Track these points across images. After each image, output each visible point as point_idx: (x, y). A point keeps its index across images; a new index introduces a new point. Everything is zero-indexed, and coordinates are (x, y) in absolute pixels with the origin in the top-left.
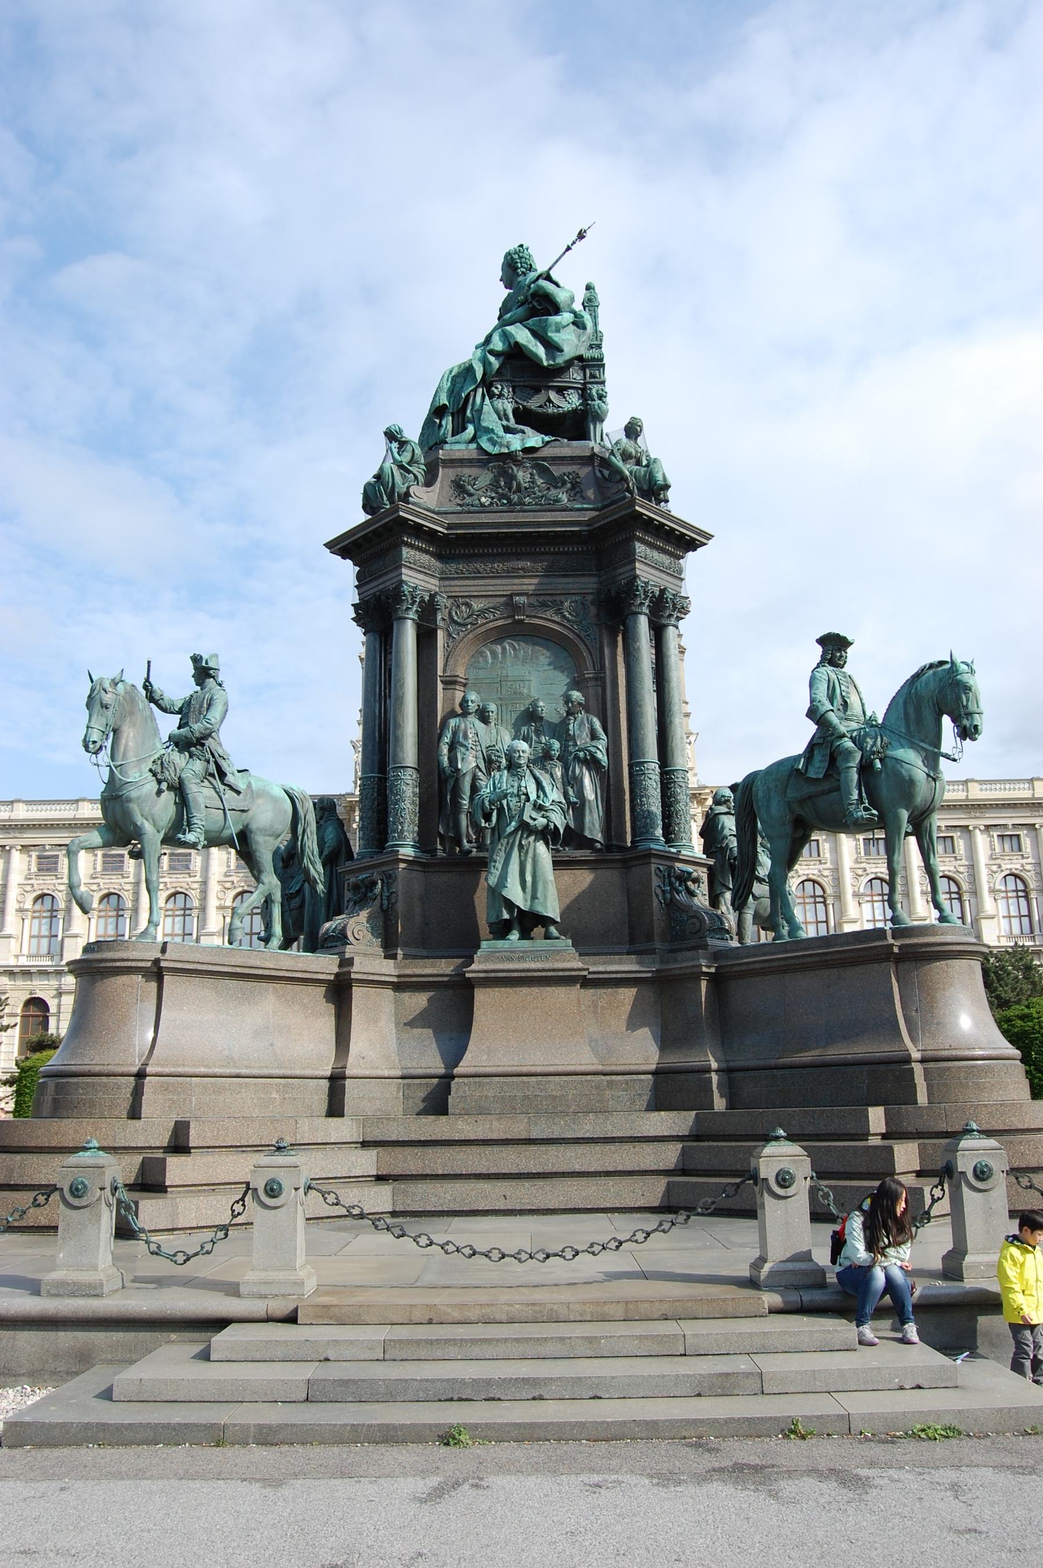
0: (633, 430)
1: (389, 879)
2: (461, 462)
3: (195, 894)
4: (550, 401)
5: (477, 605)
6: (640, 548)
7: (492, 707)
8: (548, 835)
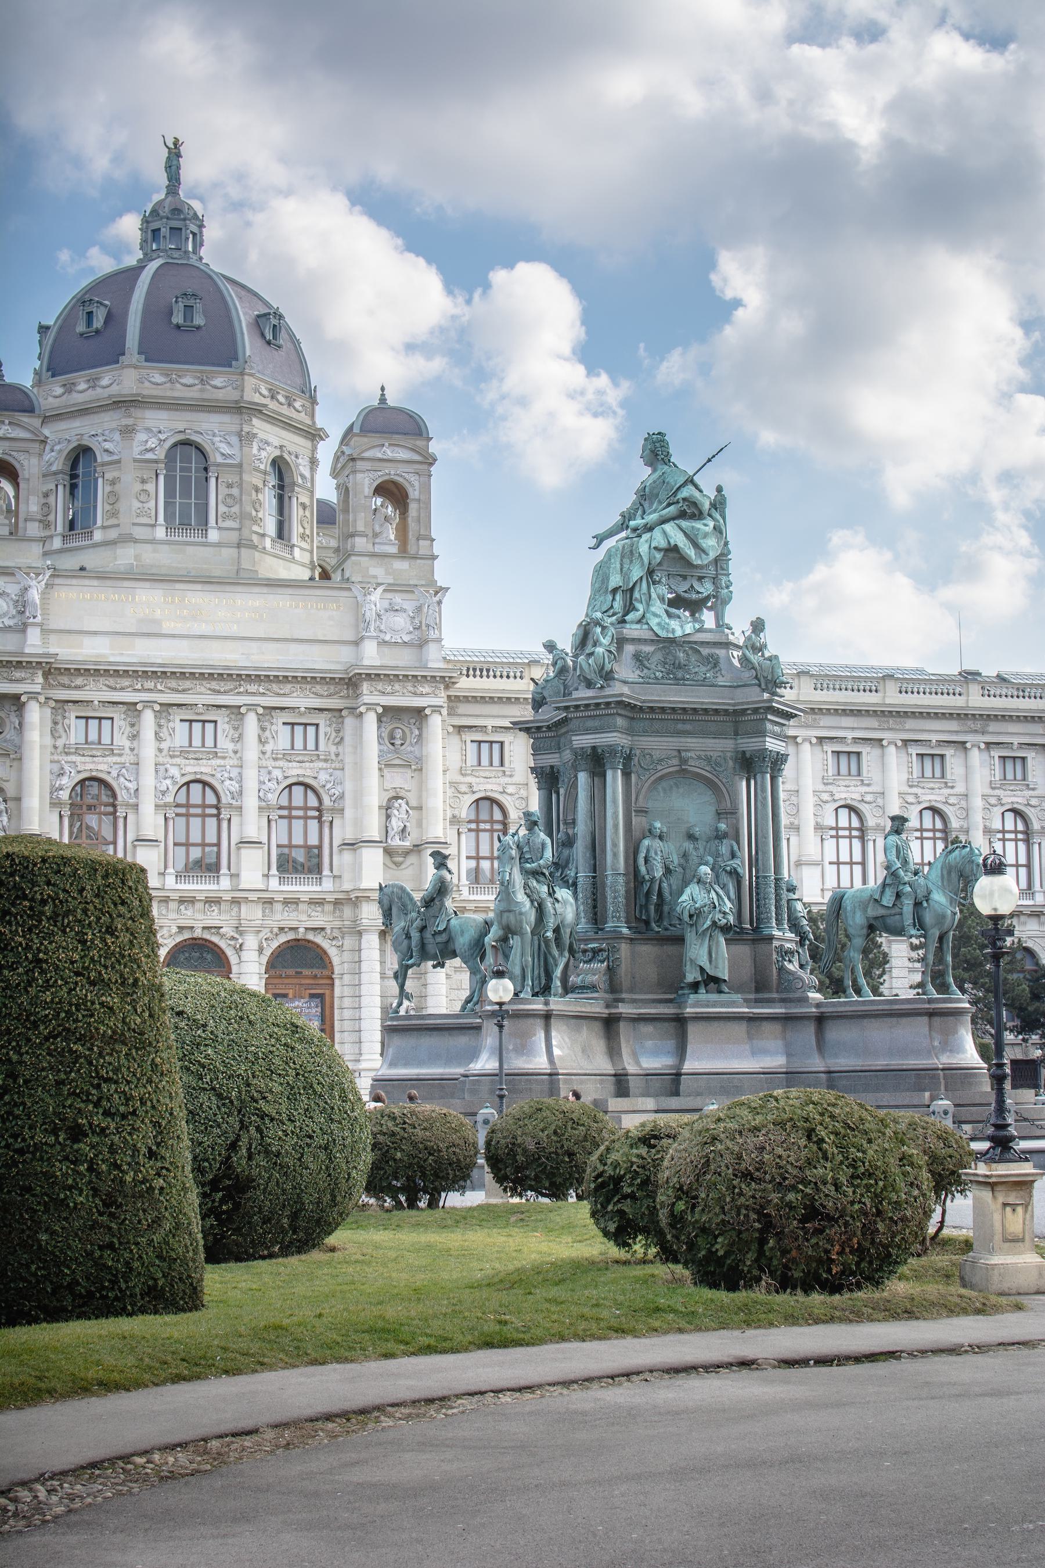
1: (614, 950)
4: (692, 586)
6: (769, 726)
8: (726, 929)
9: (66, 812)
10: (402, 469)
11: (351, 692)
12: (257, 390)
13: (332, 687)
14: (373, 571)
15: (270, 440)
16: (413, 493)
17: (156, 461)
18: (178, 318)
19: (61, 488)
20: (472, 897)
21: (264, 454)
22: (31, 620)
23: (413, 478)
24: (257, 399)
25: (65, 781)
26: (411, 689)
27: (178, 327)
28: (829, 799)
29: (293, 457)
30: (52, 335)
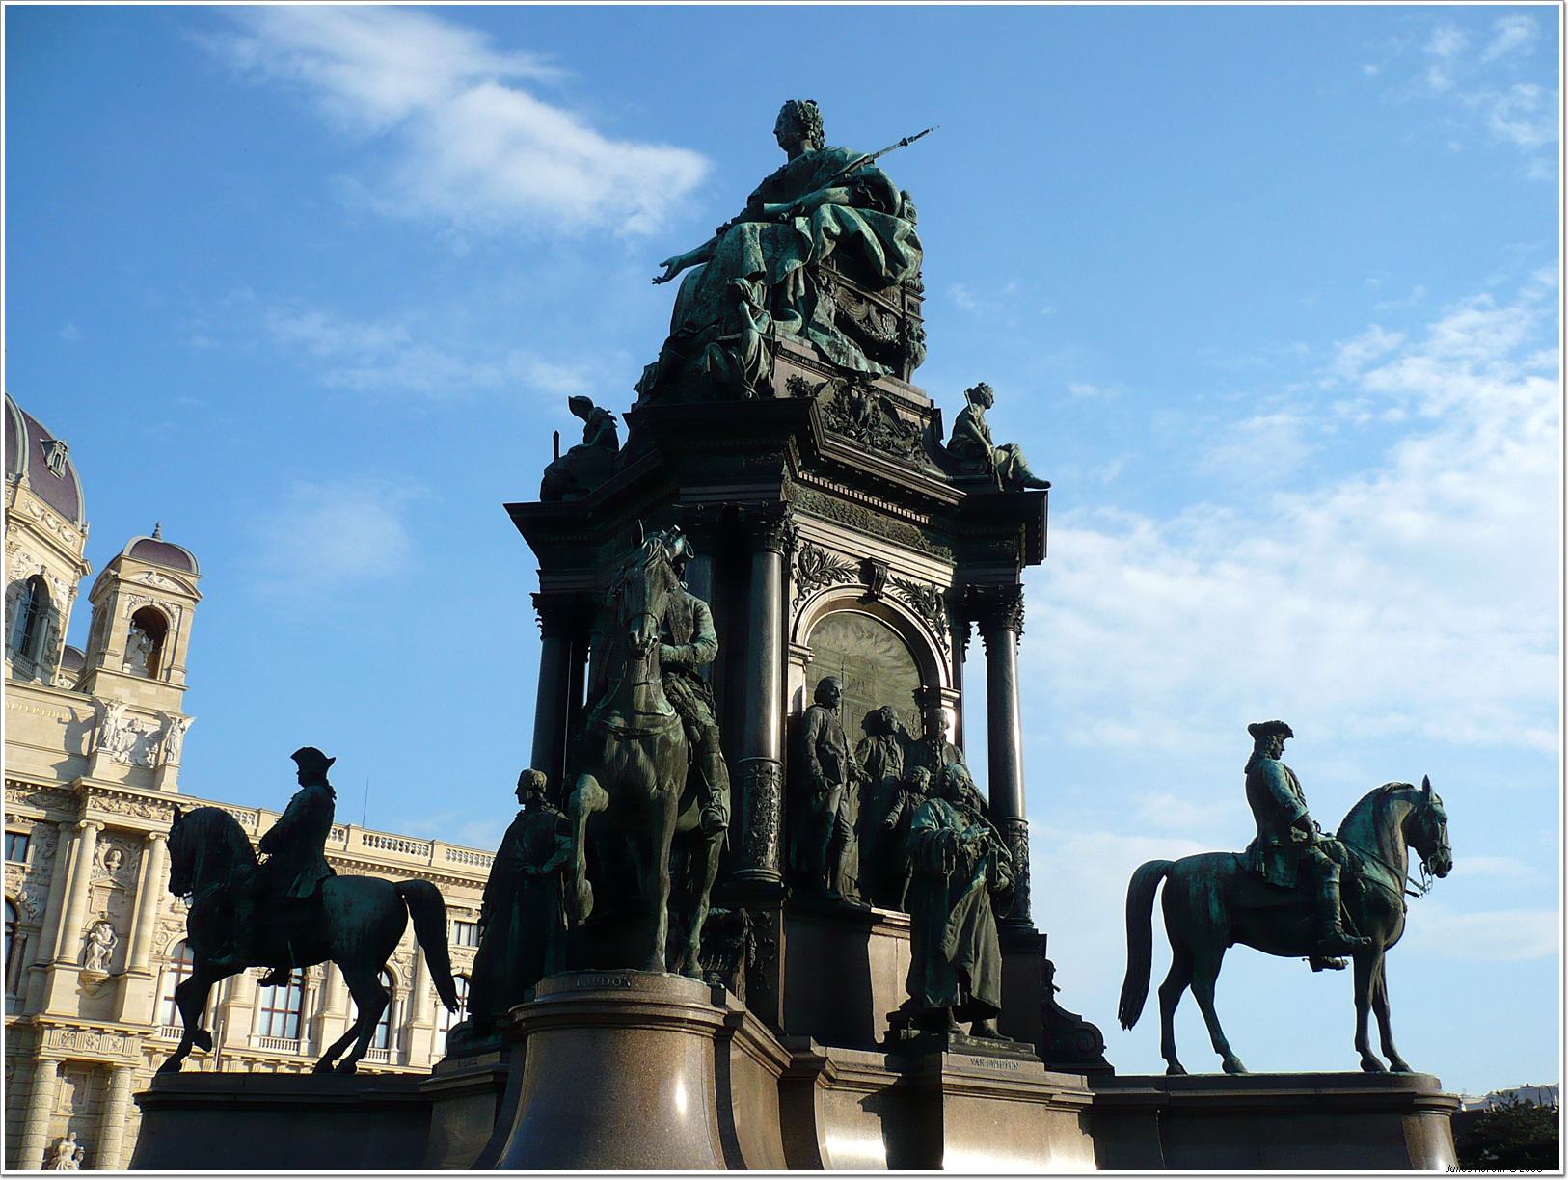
10: (166, 598)
11: (73, 806)
12: (28, 506)
13: (53, 798)
15: (32, 557)
21: (23, 567)
23: (174, 609)
29: (53, 580)
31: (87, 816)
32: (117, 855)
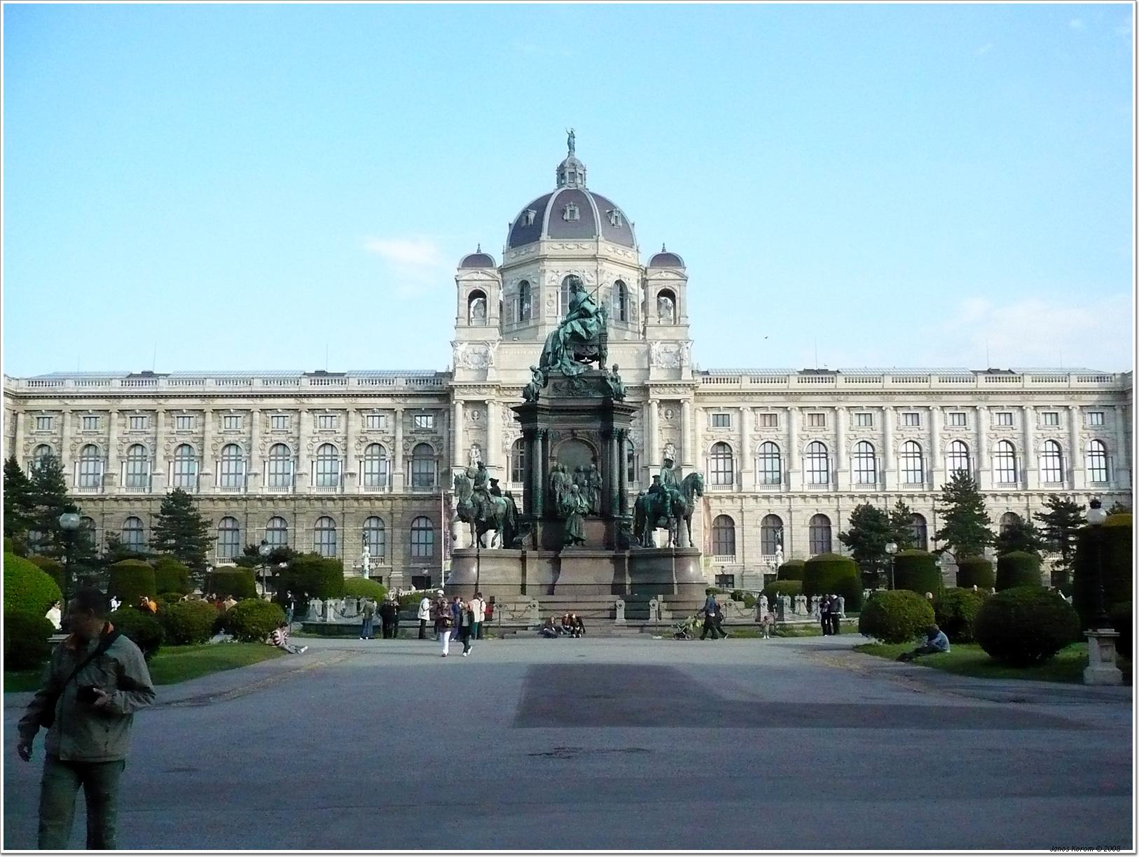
0: (615, 369)
2: (556, 378)
3: (340, 447)
4: (587, 350)
5: (561, 432)
7: (566, 467)
8: (584, 515)
9: (510, 456)
10: (671, 283)
12: (606, 249)
14: (657, 334)
15: (613, 273)
16: (677, 295)
17: (556, 286)
18: (567, 216)
19: (516, 301)
20: (714, 491)
21: (609, 279)
22: (490, 365)
23: (676, 287)
24: (606, 253)
25: (509, 440)
26: (673, 390)
27: (566, 220)
28: (853, 438)
29: (627, 280)
30: (513, 226)
31: (651, 397)
32: (670, 412)
